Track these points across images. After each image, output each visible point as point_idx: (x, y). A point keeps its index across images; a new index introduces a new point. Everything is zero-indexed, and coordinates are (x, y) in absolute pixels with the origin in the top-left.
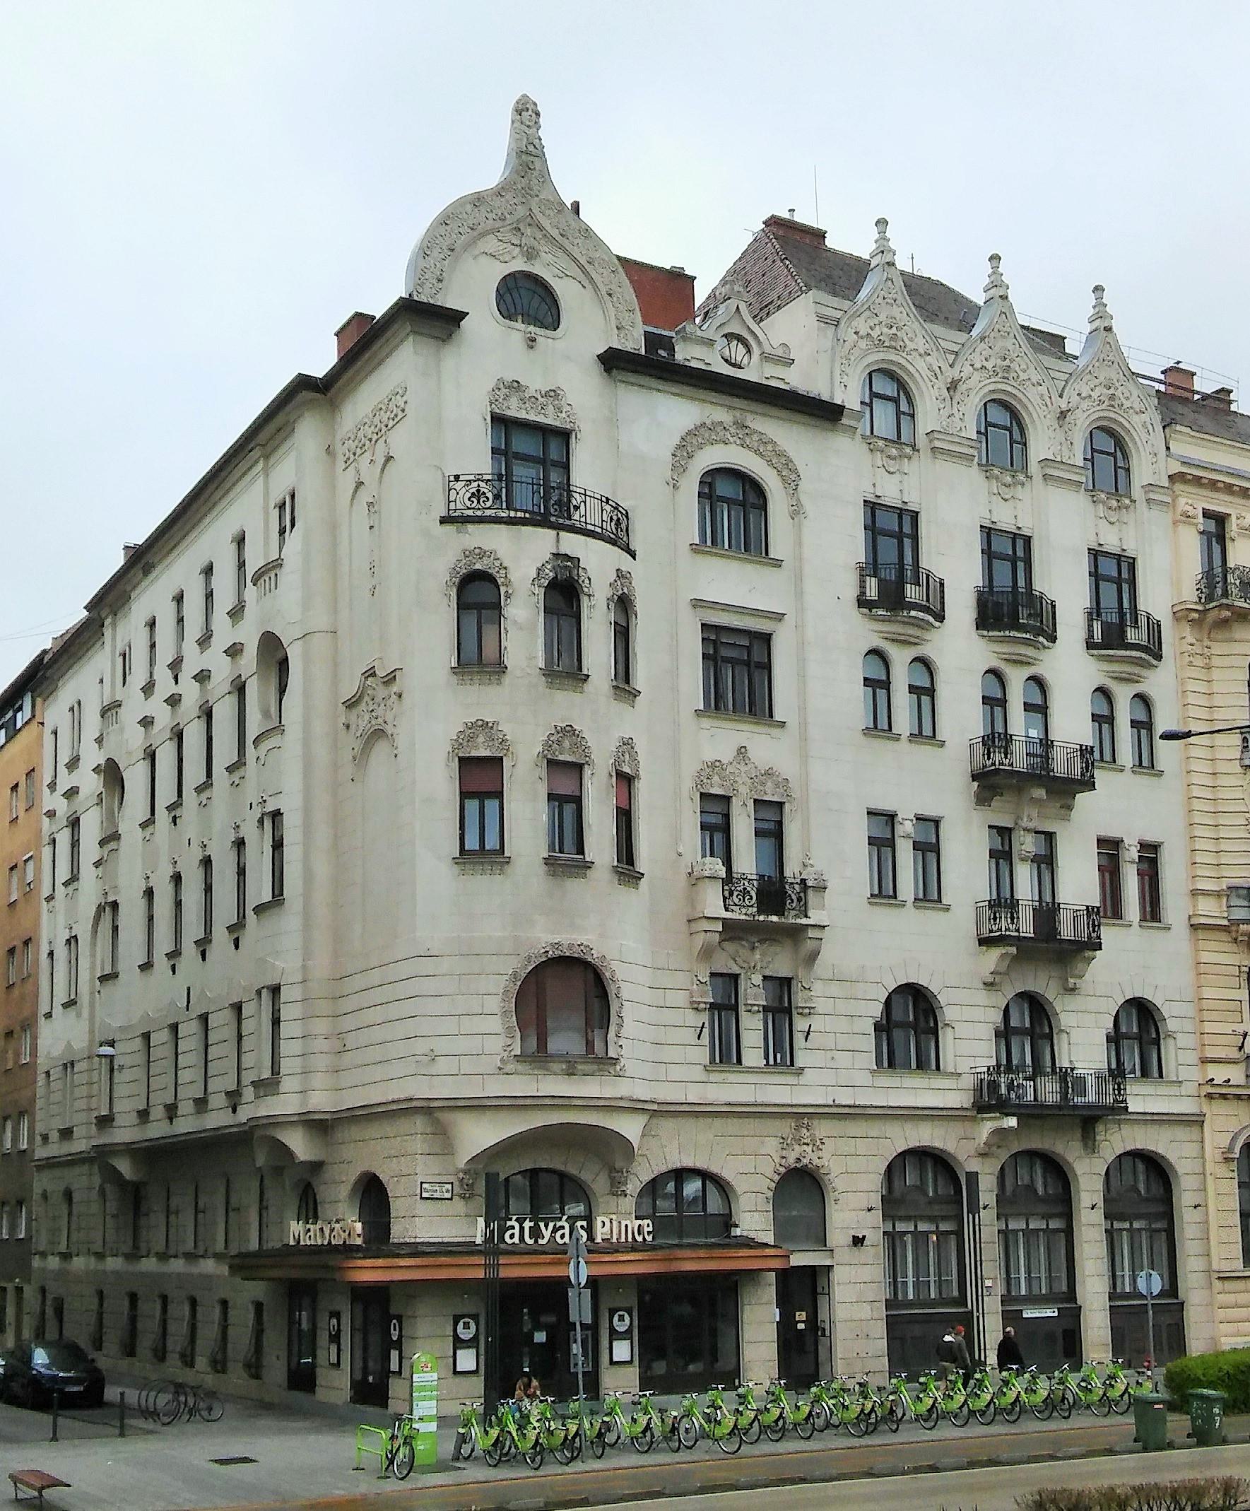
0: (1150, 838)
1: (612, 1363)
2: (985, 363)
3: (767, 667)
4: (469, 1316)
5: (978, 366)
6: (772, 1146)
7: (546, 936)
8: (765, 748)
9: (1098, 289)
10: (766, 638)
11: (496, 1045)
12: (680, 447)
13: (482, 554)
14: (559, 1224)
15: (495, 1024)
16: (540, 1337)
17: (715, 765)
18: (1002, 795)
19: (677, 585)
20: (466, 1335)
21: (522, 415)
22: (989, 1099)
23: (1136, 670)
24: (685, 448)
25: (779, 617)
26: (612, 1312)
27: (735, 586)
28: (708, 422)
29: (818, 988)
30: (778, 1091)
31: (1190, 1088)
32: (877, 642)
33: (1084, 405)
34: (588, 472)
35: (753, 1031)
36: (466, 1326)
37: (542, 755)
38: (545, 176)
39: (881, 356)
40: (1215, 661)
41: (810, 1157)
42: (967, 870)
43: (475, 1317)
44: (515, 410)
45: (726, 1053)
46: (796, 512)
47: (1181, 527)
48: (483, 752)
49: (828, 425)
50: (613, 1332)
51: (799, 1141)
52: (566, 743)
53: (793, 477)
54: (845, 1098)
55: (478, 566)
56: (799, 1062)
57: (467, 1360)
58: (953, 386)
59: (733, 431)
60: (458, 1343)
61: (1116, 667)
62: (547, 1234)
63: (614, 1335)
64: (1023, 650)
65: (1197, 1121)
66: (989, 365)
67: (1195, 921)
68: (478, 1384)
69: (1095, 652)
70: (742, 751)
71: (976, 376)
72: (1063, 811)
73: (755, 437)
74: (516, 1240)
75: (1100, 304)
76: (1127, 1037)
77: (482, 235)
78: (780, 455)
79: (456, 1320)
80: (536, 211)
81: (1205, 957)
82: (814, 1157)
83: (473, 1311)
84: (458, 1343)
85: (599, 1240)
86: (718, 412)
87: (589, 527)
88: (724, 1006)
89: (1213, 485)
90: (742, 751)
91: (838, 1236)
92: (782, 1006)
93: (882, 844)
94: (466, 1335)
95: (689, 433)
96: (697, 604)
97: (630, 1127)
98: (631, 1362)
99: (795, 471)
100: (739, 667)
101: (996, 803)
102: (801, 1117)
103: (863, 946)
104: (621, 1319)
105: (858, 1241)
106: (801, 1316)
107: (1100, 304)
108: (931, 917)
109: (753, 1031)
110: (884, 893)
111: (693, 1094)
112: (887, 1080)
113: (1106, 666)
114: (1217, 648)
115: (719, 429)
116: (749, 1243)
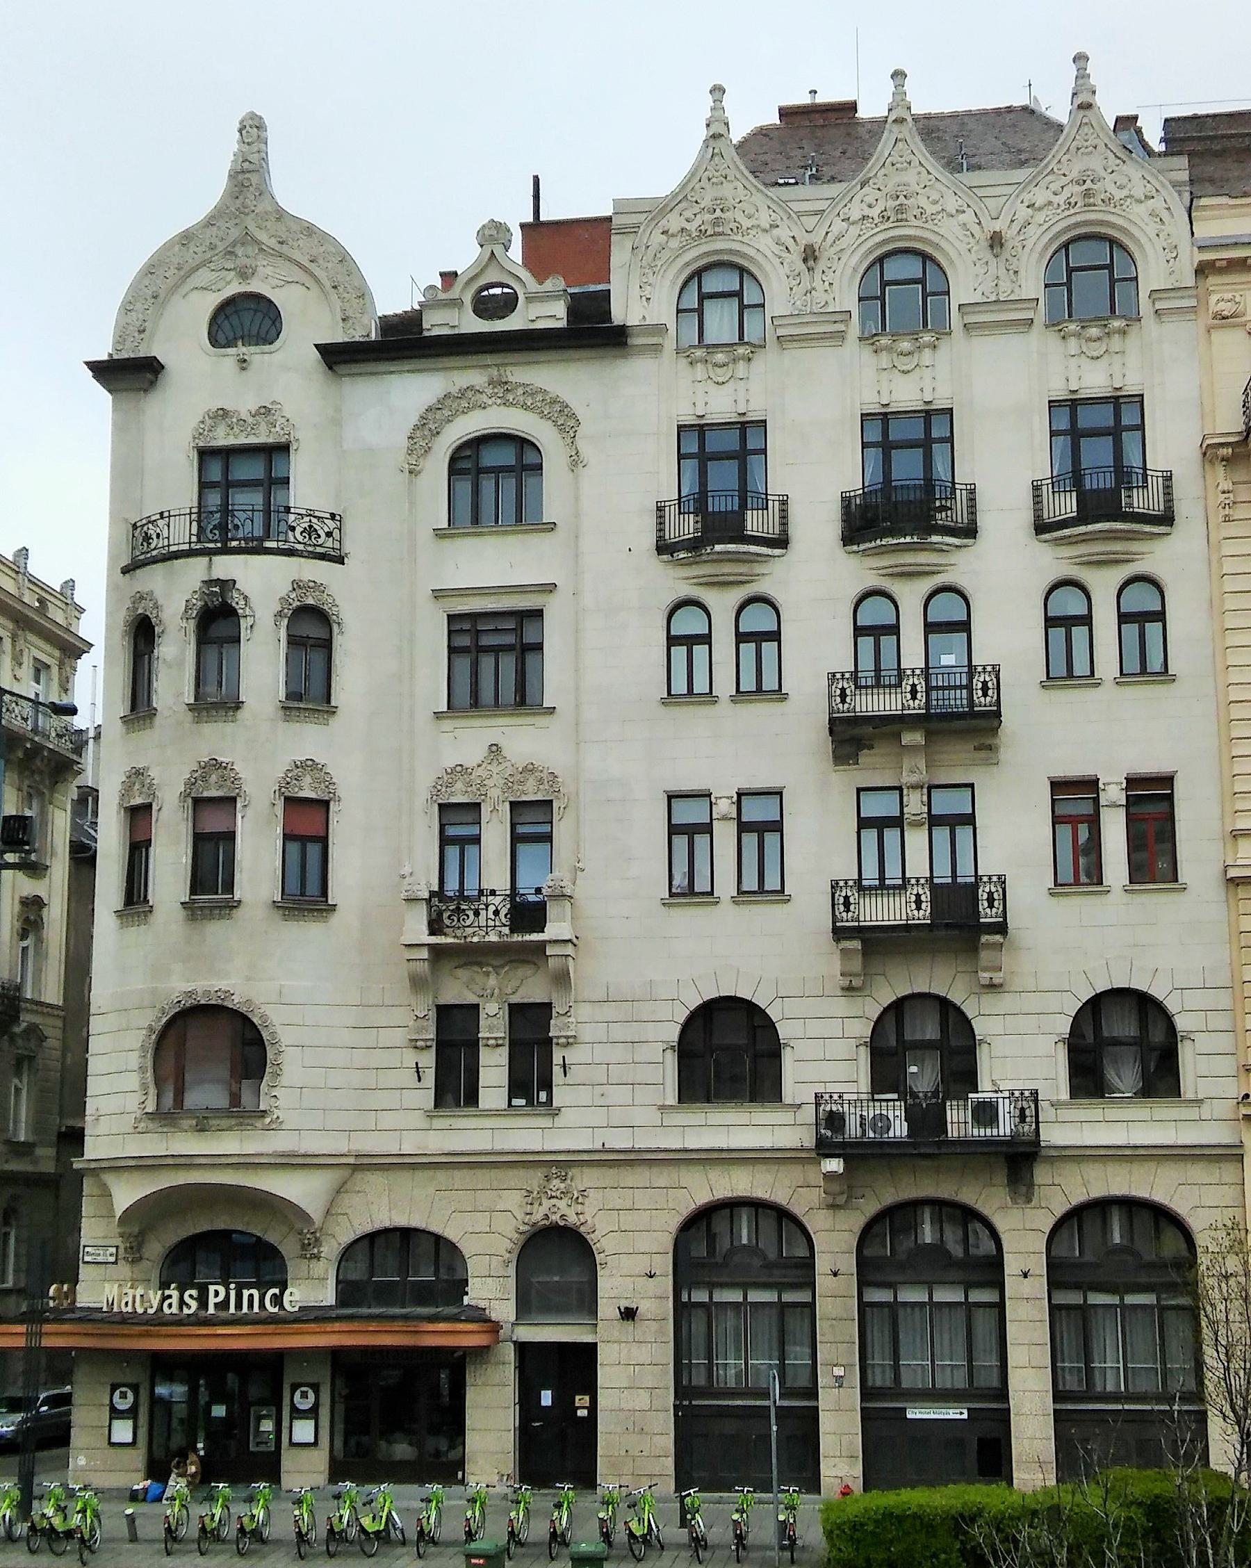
1: (292, 1444)
2: (867, 211)
3: (539, 647)
4: (124, 1385)
6: (513, 1200)
7: (184, 984)
8: (523, 740)
9: (1080, 59)
12: (421, 425)
15: (133, 1081)
16: (219, 1411)
17: (460, 771)
18: (871, 747)
20: (123, 1405)
21: (231, 441)
23: (1118, 546)
24: (427, 426)
25: (550, 588)
27: (492, 565)
29: (583, 1012)
30: (526, 1134)
31: (1224, 1109)
33: (1040, 217)
35: (494, 1070)
37: (185, 795)
41: (565, 1212)
42: (820, 844)
44: (222, 438)
46: (576, 462)
47: (1216, 335)
48: (307, 793)
50: (294, 1409)
53: (572, 423)
54: (620, 1140)
56: (556, 1103)
57: (123, 1431)
58: (810, 255)
59: (489, 391)
60: (115, 1413)
63: (297, 1413)
64: (909, 558)
67: (1232, 873)
68: (138, 1458)
69: (1047, 536)
71: (855, 231)
72: (983, 754)
73: (520, 391)
74: (175, 1310)
77: (197, 268)
78: (554, 401)
79: (114, 1388)
83: (131, 1379)
87: (173, 549)
88: (454, 1040)
91: (607, 1309)
92: (533, 1040)
93: (686, 832)
94: (123, 1405)
95: (429, 410)
98: (315, 1444)
99: (573, 416)
101: (865, 757)
102: (558, 1165)
103: (635, 960)
104: (304, 1395)
105: (629, 1314)
108: (764, 914)
109: (494, 1070)
110: (688, 892)
111: (409, 1145)
112: (696, 1116)
116: (479, 1316)
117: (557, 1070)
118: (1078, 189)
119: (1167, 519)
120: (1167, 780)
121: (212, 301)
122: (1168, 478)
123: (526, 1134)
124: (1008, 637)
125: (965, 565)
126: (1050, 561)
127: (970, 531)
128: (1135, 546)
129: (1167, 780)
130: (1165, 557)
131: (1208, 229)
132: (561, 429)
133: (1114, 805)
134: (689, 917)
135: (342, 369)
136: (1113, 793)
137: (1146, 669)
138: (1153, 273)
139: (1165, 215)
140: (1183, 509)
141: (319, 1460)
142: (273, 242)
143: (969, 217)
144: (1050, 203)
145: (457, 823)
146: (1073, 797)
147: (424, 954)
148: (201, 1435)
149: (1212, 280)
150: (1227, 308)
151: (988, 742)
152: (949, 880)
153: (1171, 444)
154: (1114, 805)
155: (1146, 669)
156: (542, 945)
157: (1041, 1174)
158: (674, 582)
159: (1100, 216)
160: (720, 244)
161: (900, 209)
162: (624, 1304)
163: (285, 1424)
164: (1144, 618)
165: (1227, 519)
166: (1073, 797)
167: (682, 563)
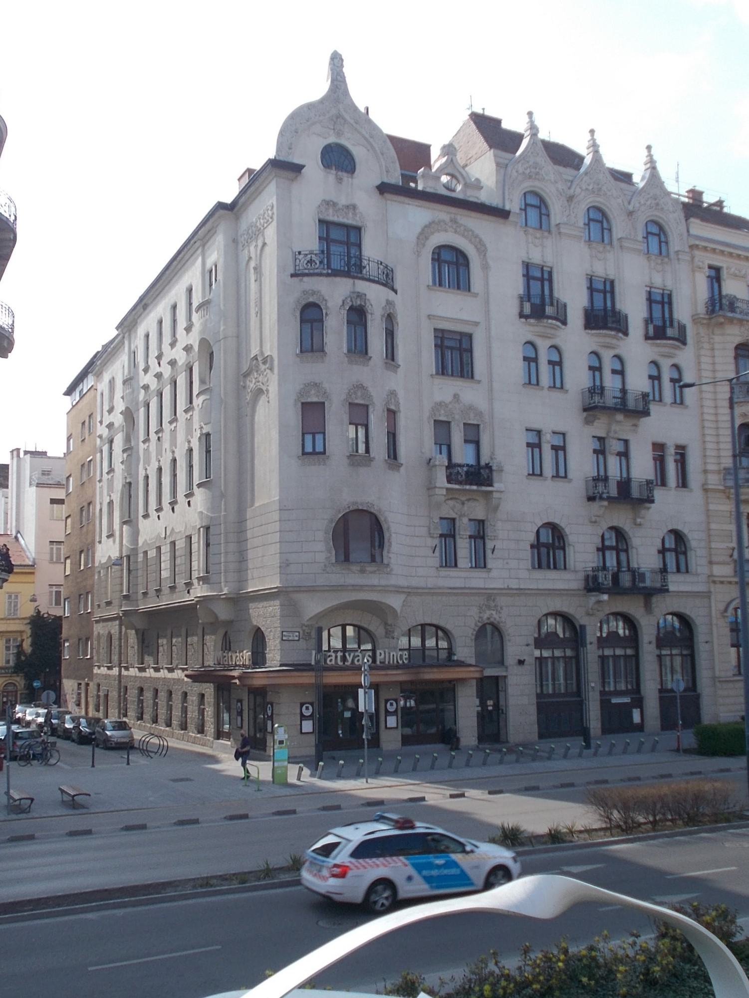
0: (681, 442)
3: (470, 351)
5: (584, 188)
6: (474, 611)
7: (348, 498)
8: (470, 394)
10: (470, 336)
11: (321, 558)
12: (421, 233)
13: (314, 293)
14: (357, 654)
15: (320, 546)
17: (440, 404)
19: (421, 309)
20: (307, 713)
22: (592, 585)
23: (672, 351)
25: (476, 324)
26: (386, 701)
27: (452, 309)
28: (436, 220)
29: (499, 525)
30: (477, 580)
32: (530, 337)
33: (643, 208)
34: (372, 249)
35: (464, 547)
36: (307, 708)
38: (346, 93)
39: (531, 184)
40: (717, 346)
41: (495, 617)
43: (312, 704)
45: (450, 561)
46: (486, 267)
48: (315, 399)
49: (501, 221)
50: (387, 711)
51: (489, 608)
52: (359, 394)
54: (514, 584)
55: (311, 300)
56: (489, 565)
58: (570, 199)
59: (450, 224)
60: (303, 717)
61: (662, 350)
62: (350, 659)
63: (388, 713)
65: (707, 595)
66: (590, 188)
68: (312, 739)
69: (649, 341)
70: (456, 397)
71: (583, 194)
72: (634, 428)
73: (462, 228)
74: (333, 662)
75: (650, 156)
78: (477, 236)
79: (302, 705)
80: (342, 110)
82: (497, 617)
83: (310, 700)
84: (303, 717)
85: (378, 663)
86: (442, 213)
89: (714, 251)
90: (456, 397)
91: (510, 660)
92: (480, 534)
93: (535, 446)
94: (307, 713)
95: (426, 226)
96: (429, 317)
97: (395, 602)
98: (397, 728)
99: (484, 246)
100: (455, 353)
102: (490, 597)
103: (525, 501)
104: (391, 704)
105: (521, 662)
106: (490, 703)
107: (650, 156)
109: (464, 547)
110: (536, 473)
111: (431, 583)
112: (539, 574)
113: (656, 349)
114: (717, 339)
115: (442, 223)
116: (461, 664)
117: (489, 552)
121: (322, 143)
123: (477, 580)
130: (686, 357)
132: (478, 250)
134: (535, 483)
135: (387, 196)
138: (676, 244)
140: (690, 339)
141: (397, 735)
142: (352, 122)
143: (620, 201)
145: (442, 428)
147: (444, 492)
148: (340, 726)
153: (683, 312)
156: (491, 492)
158: (527, 331)
160: (537, 183)
161: (600, 189)
162: (518, 658)
163: (382, 718)
167: (531, 325)
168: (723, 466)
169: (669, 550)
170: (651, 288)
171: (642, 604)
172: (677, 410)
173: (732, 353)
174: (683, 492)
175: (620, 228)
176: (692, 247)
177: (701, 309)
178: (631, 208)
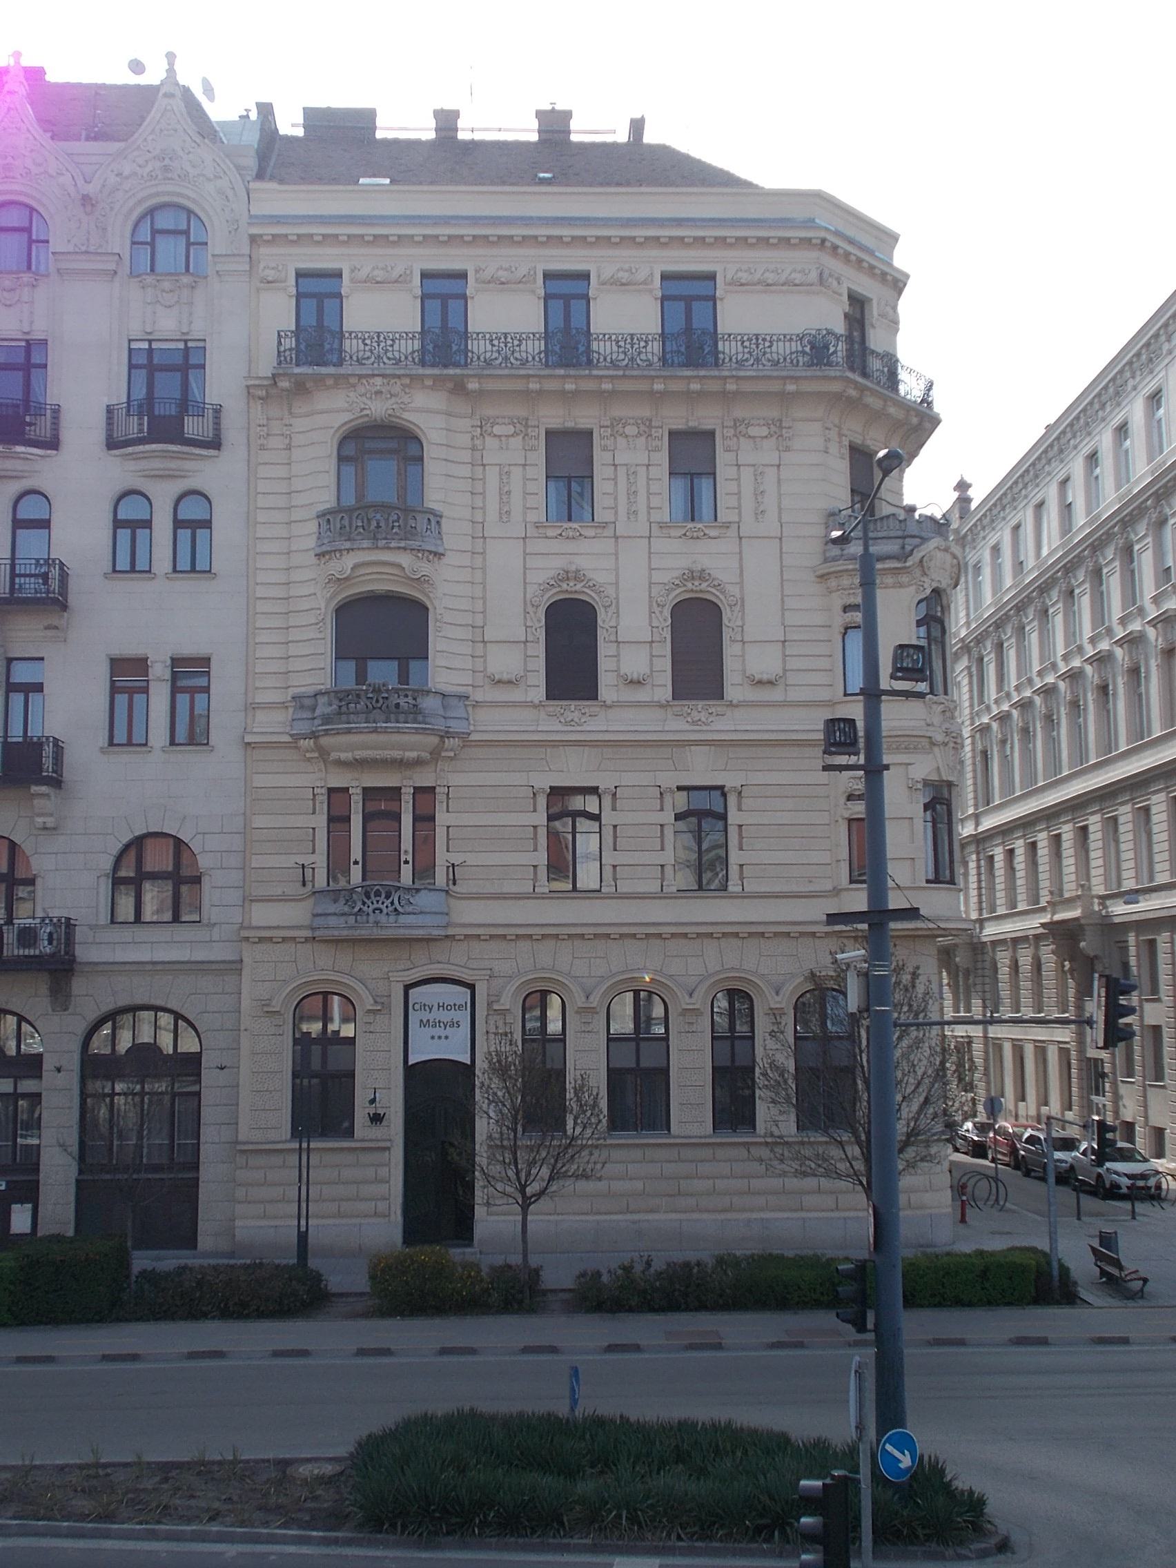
23: (173, 464)
61: (144, 464)
65: (235, 967)
76: (154, 876)
81: (259, 781)
113: (132, 465)
114: (300, 424)
118: (158, 164)
119: (215, 444)
120: (206, 661)
122: (218, 411)
124: (80, 537)
125: (48, 472)
126: (118, 472)
127: (53, 444)
128: (188, 465)
129: (206, 661)
131: (262, 207)
133: (159, 680)
136: (160, 671)
137: (193, 567)
138: (218, 242)
139: (230, 193)
144: (135, 174)
146: (127, 674)
149: (264, 250)
150: (271, 274)
151: (56, 623)
152: (20, 740)
153: (223, 383)
154: (159, 680)
155: (193, 567)
157: (78, 986)
159: (178, 190)
164: (193, 525)
165: (262, 448)
166: (127, 674)
168: (291, 692)
169: (154, 876)
170: (150, 341)
171: (44, 989)
172: (185, 584)
173: (331, 449)
174: (190, 758)
175: (62, 234)
176: (253, 239)
177: (266, 366)
178: (90, 189)
